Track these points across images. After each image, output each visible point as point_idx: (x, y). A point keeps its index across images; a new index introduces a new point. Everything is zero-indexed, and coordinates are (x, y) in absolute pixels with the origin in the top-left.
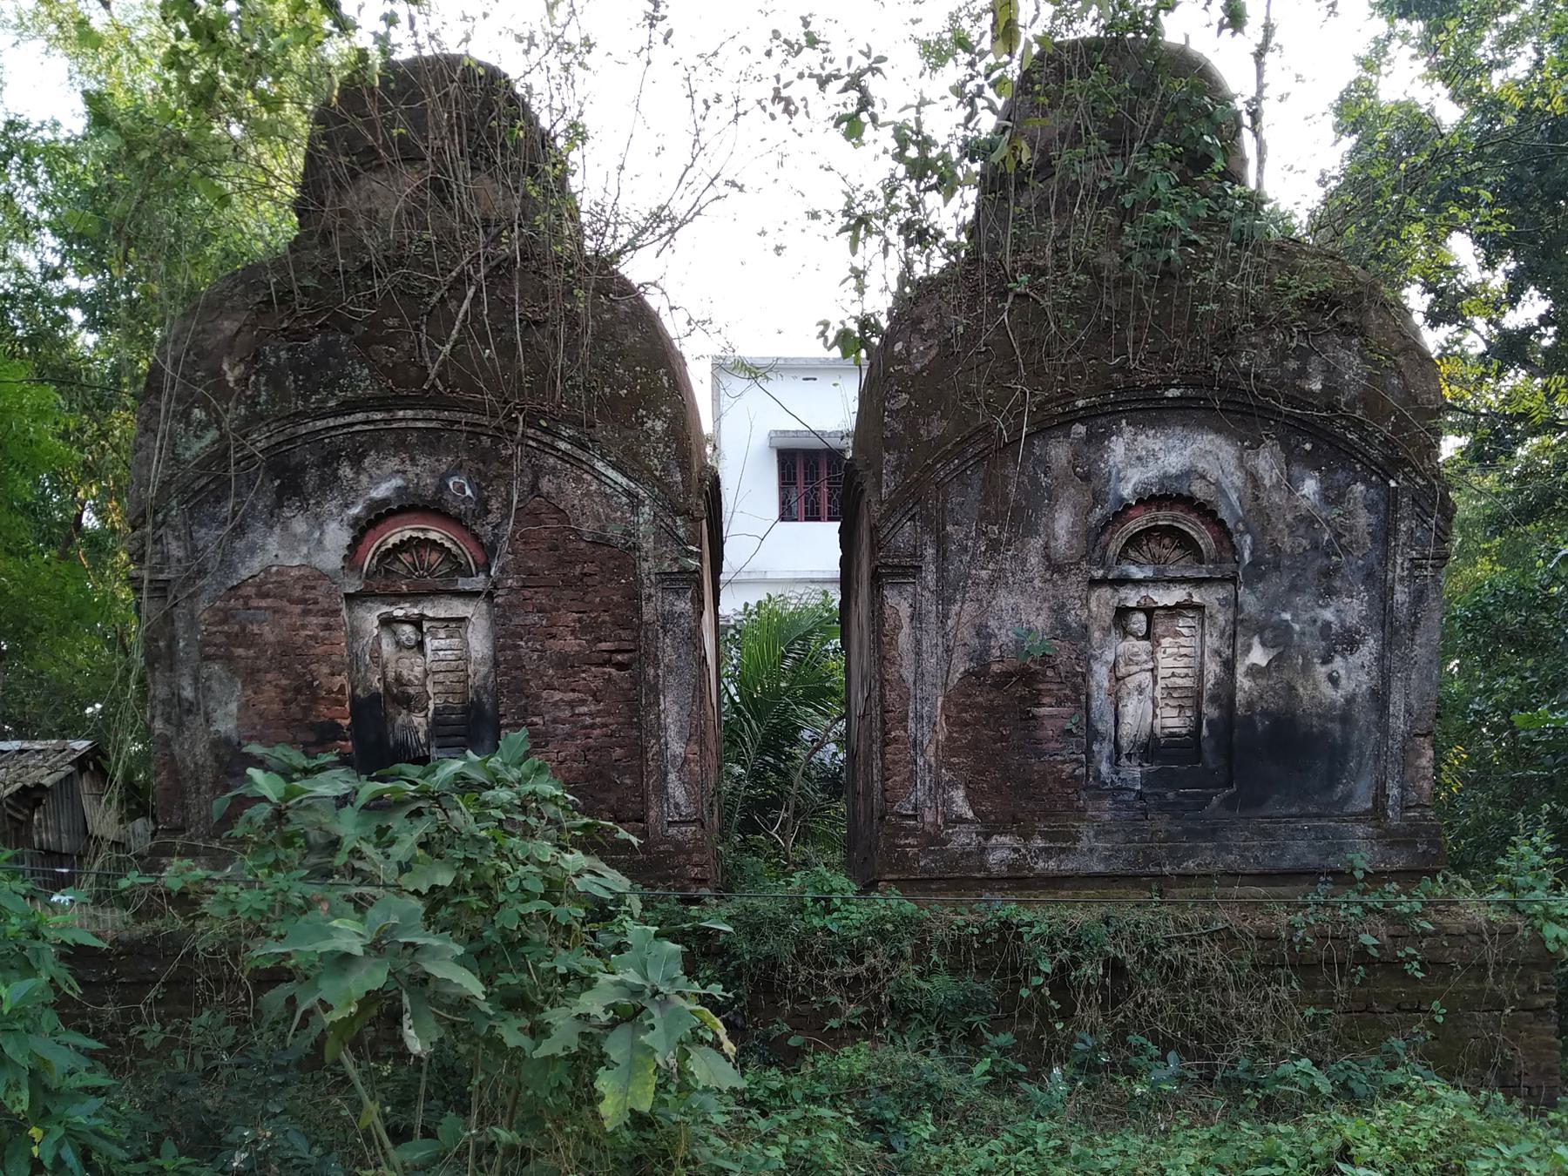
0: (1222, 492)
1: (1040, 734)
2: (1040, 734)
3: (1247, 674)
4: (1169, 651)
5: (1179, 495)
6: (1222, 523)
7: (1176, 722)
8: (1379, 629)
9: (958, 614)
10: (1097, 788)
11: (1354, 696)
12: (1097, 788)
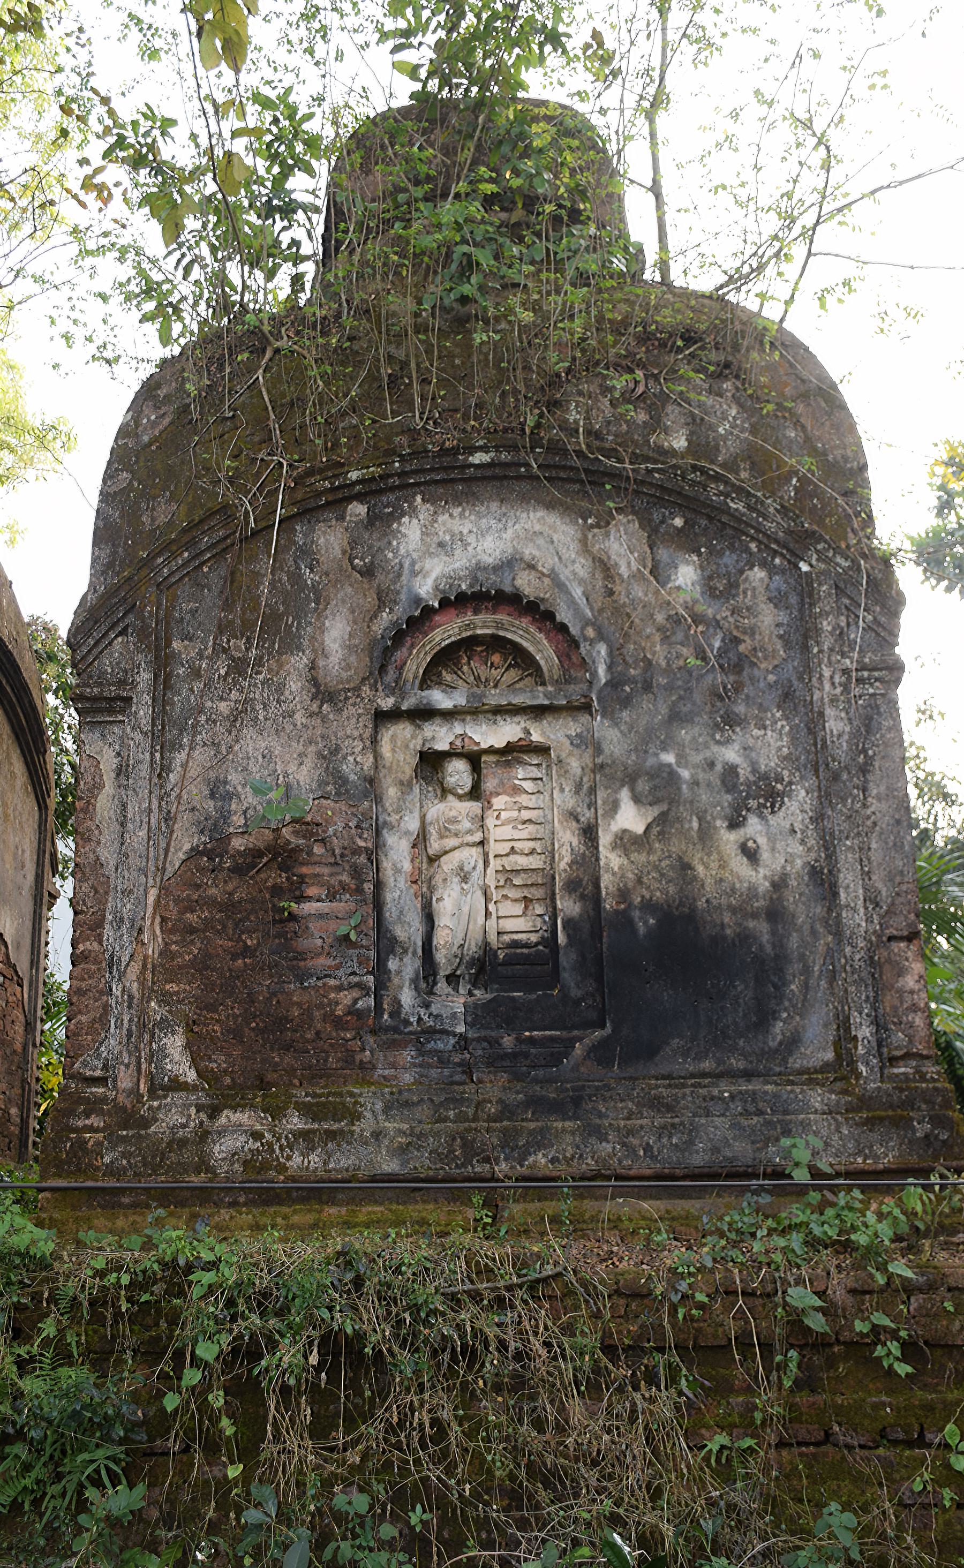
0: (559, 585)
1: (303, 944)
2: (303, 944)
3: (614, 846)
5: (500, 593)
6: (563, 628)
7: (521, 924)
8: (810, 774)
9: (185, 766)
10: (396, 1030)
11: (784, 877)
12: (396, 1030)
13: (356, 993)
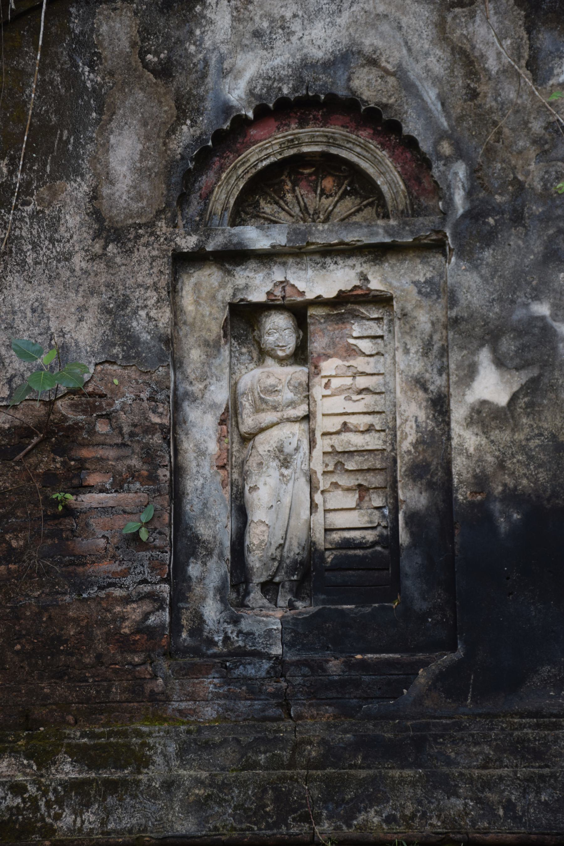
3: (470, 422)
4: (336, 383)
5: (332, 98)
12: (196, 651)
13: (146, 606)
